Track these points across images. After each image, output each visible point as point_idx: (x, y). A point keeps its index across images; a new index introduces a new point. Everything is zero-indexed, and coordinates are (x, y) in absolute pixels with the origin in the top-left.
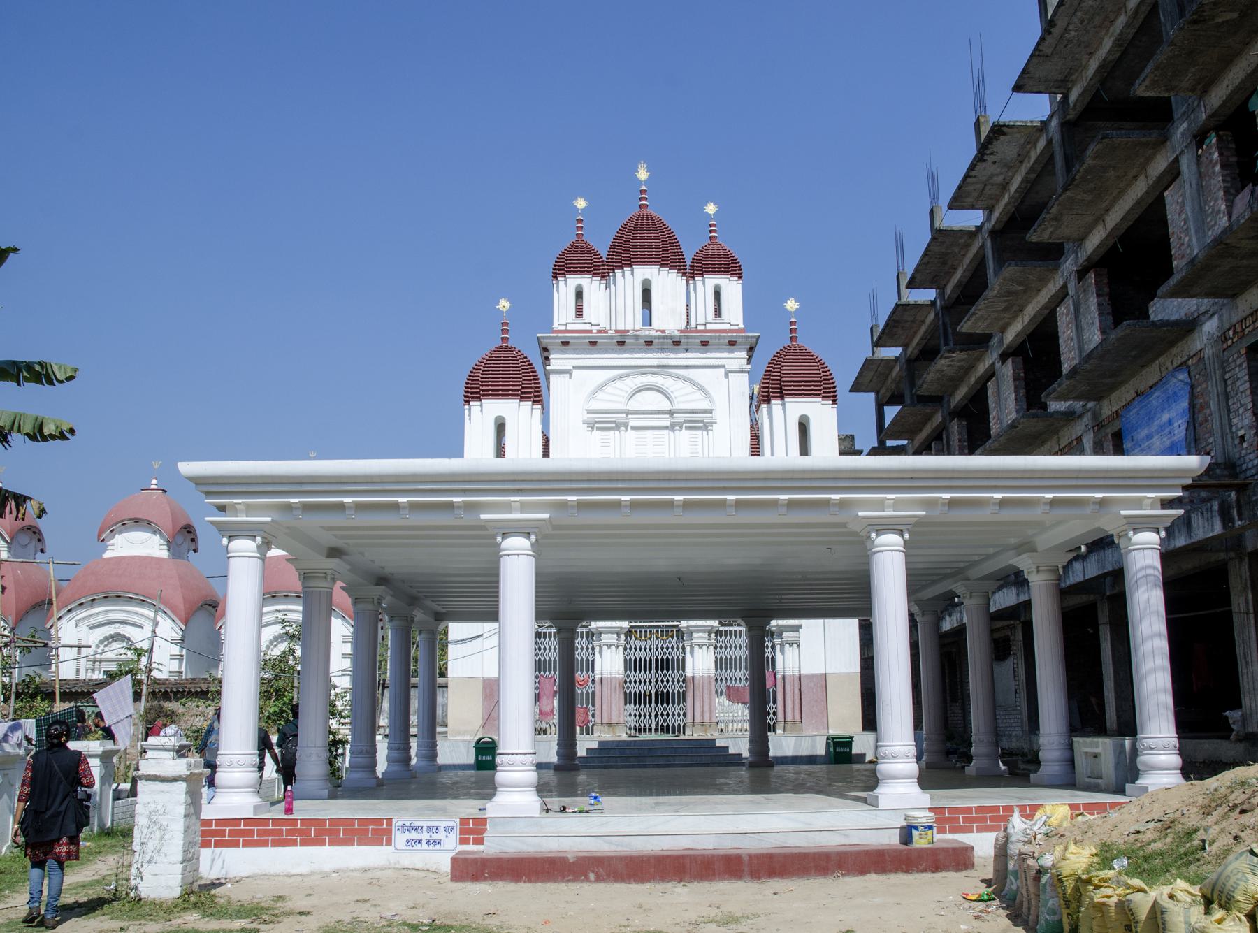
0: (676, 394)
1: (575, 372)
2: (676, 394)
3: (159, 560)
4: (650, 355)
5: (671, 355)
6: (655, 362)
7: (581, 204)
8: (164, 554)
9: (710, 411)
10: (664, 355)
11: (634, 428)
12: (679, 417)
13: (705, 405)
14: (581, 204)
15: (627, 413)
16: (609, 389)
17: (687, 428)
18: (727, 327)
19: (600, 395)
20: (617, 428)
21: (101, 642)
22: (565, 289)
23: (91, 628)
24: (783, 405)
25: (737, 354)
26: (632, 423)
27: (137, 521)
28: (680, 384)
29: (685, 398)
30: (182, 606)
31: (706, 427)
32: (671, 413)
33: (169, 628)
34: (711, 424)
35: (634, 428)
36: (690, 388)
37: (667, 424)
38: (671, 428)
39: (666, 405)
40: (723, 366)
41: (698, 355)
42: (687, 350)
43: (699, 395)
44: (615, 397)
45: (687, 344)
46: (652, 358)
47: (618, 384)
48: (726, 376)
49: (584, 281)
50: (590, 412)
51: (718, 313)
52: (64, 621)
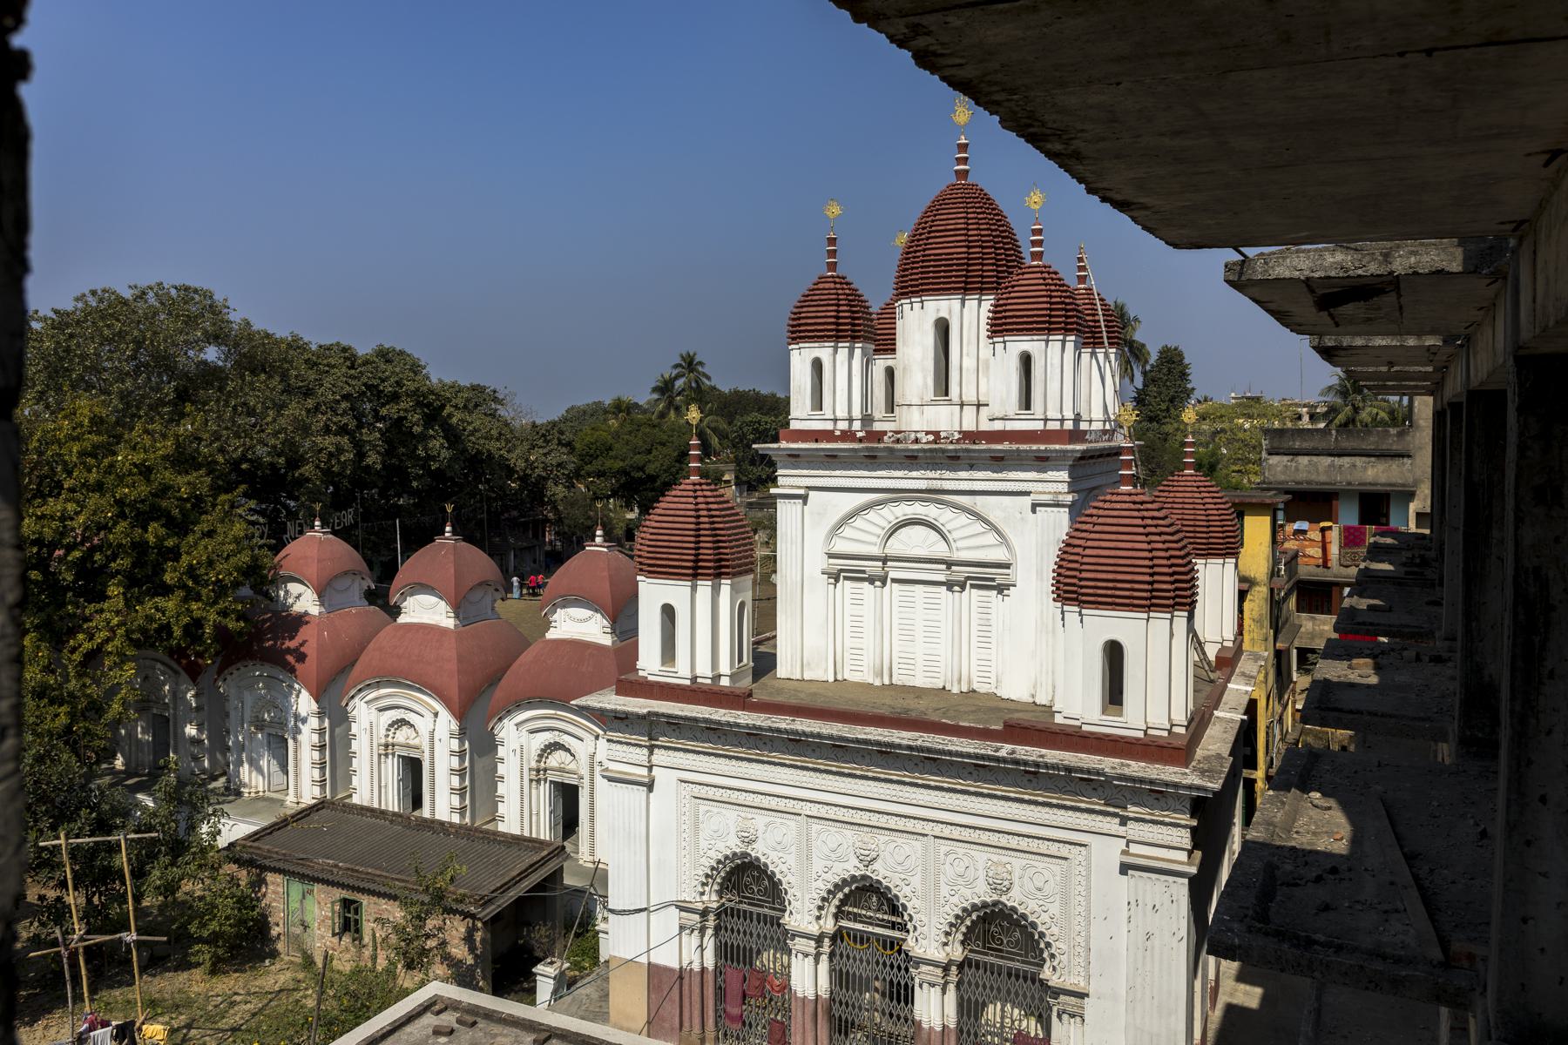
0: (955, 535)
1: (812, 493)
2: (955, 535)
3: (442, 631)
4: (914, 474)
5: (948, 474)
6: (922, 485)
7: (834, 210)
8: (449, 622)
9: (1007, 566)
10: (937, 474)
11: (894, 581)
12: (961, 572)
13: (999, 555)
14: (834, 210)
15: (885, 560)
16: (858, 522)
17: (972, 586)
18: (1039, 426)
19: (847, 531)
20: (871, 580)
21: (391, 725)
22: (801, 359)
23: (381, 710)
24: (1080, 614)
25: (1051, 475)
26: (892, 575)
27: (421, 585)
28: (964, 519)
29: (970, 542)
30: (456, 699)
31: (1001, 589)
32: (949, 564)
33: (446, 723)
34: (1008, 587)
35: (894, 581)
36: (979, 527)
37: (942, 578)
38: (949, 585)
39: (939, 549)
40: (1027, 493)
41: (989, 474)
42: (971, 467)
43: (991, 538)
44: (864, 537)
45: (971, 458)
46: (916, 479)
47: (872, 515)
48: (1034, 511)
49: (824, 352)
50: (831, 556)
51: (1026, 402)
52: (356, 699)
